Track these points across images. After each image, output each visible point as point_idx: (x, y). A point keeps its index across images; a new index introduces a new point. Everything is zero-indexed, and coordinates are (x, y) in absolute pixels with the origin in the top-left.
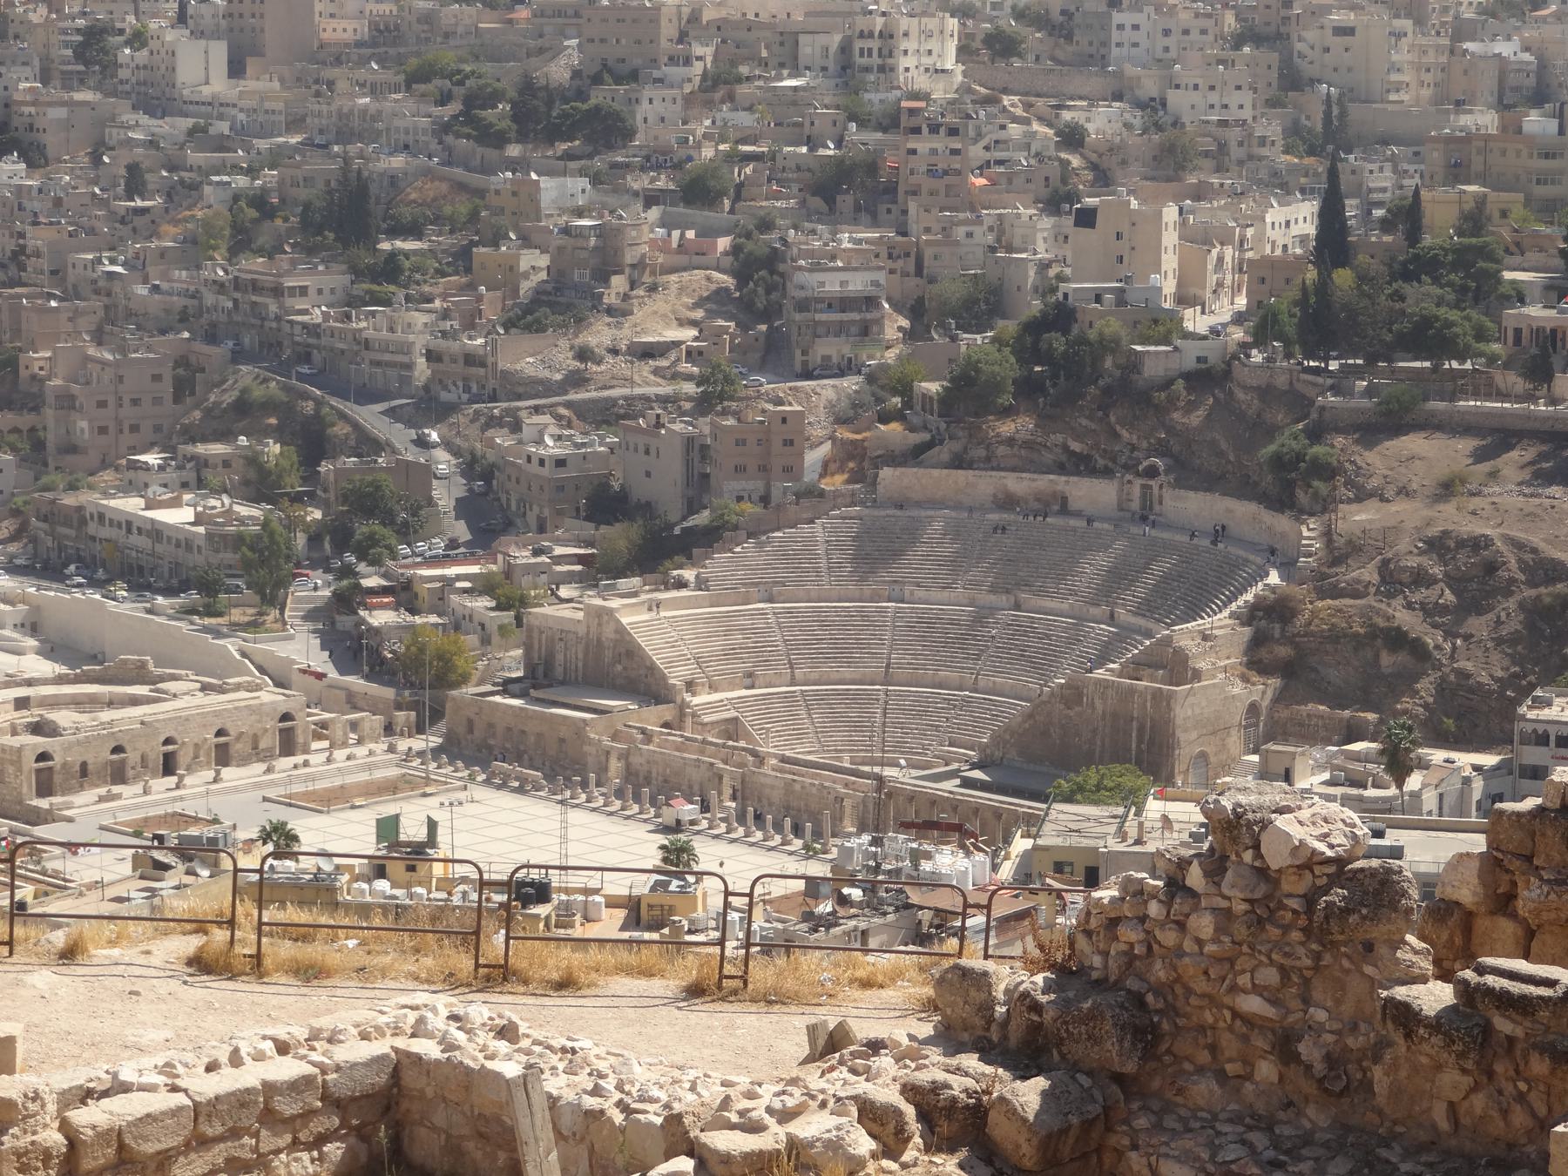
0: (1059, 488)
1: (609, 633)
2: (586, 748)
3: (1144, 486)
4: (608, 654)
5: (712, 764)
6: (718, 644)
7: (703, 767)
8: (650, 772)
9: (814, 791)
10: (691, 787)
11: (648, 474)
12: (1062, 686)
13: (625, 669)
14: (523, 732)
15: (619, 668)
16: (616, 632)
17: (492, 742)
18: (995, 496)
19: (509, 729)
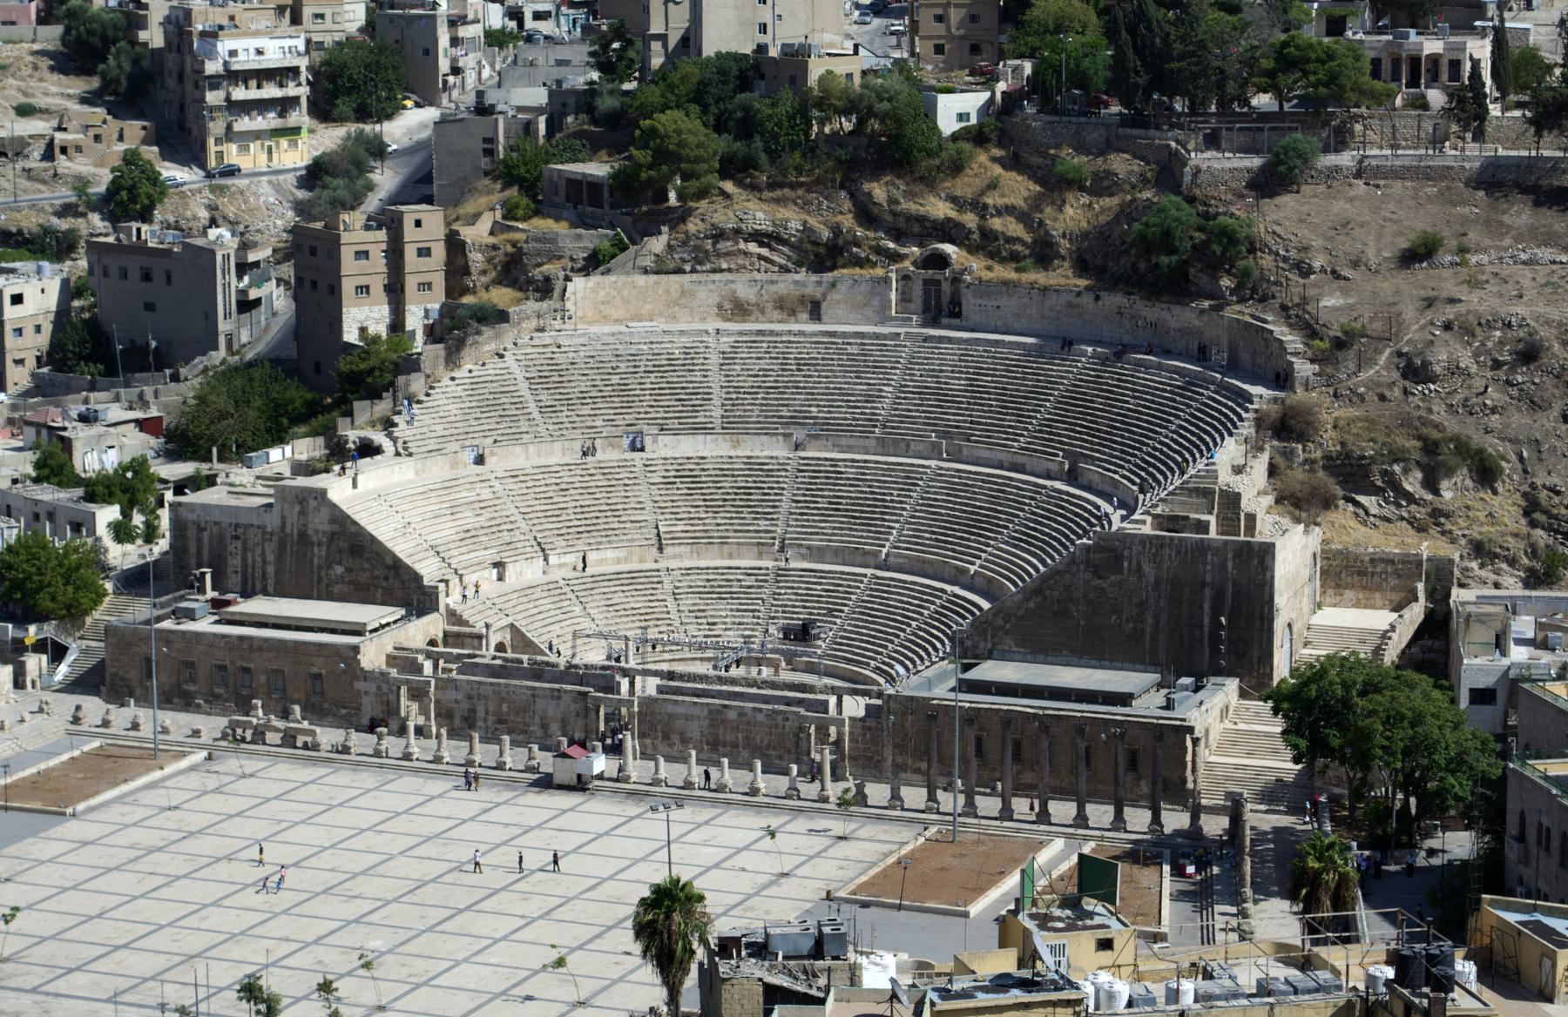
0: (809, 291)
1: (319, 523)
2: (360, 685)
3: (926, 282)
4: (319, 554)
5: (586, 694)
6: (446, 531)
7: (566, 699)
8: (473, 711)
9: (760, 717)
10: (545, 727)
11: (149, 307)
12: (1088, 548)
13: (349, 570)
14: (247, 670)
15: (339, 570)
16: (333, 521)
17: (192, 688)
18: (720, 307)
19: (222, 668)
